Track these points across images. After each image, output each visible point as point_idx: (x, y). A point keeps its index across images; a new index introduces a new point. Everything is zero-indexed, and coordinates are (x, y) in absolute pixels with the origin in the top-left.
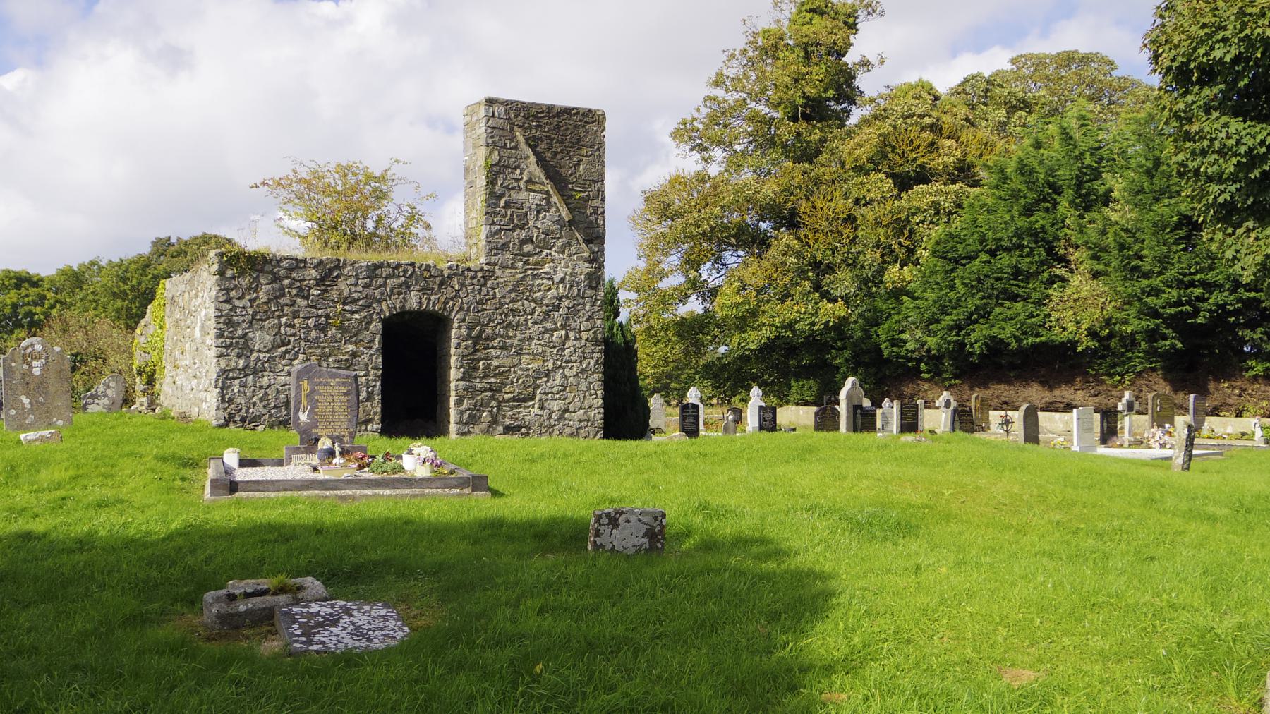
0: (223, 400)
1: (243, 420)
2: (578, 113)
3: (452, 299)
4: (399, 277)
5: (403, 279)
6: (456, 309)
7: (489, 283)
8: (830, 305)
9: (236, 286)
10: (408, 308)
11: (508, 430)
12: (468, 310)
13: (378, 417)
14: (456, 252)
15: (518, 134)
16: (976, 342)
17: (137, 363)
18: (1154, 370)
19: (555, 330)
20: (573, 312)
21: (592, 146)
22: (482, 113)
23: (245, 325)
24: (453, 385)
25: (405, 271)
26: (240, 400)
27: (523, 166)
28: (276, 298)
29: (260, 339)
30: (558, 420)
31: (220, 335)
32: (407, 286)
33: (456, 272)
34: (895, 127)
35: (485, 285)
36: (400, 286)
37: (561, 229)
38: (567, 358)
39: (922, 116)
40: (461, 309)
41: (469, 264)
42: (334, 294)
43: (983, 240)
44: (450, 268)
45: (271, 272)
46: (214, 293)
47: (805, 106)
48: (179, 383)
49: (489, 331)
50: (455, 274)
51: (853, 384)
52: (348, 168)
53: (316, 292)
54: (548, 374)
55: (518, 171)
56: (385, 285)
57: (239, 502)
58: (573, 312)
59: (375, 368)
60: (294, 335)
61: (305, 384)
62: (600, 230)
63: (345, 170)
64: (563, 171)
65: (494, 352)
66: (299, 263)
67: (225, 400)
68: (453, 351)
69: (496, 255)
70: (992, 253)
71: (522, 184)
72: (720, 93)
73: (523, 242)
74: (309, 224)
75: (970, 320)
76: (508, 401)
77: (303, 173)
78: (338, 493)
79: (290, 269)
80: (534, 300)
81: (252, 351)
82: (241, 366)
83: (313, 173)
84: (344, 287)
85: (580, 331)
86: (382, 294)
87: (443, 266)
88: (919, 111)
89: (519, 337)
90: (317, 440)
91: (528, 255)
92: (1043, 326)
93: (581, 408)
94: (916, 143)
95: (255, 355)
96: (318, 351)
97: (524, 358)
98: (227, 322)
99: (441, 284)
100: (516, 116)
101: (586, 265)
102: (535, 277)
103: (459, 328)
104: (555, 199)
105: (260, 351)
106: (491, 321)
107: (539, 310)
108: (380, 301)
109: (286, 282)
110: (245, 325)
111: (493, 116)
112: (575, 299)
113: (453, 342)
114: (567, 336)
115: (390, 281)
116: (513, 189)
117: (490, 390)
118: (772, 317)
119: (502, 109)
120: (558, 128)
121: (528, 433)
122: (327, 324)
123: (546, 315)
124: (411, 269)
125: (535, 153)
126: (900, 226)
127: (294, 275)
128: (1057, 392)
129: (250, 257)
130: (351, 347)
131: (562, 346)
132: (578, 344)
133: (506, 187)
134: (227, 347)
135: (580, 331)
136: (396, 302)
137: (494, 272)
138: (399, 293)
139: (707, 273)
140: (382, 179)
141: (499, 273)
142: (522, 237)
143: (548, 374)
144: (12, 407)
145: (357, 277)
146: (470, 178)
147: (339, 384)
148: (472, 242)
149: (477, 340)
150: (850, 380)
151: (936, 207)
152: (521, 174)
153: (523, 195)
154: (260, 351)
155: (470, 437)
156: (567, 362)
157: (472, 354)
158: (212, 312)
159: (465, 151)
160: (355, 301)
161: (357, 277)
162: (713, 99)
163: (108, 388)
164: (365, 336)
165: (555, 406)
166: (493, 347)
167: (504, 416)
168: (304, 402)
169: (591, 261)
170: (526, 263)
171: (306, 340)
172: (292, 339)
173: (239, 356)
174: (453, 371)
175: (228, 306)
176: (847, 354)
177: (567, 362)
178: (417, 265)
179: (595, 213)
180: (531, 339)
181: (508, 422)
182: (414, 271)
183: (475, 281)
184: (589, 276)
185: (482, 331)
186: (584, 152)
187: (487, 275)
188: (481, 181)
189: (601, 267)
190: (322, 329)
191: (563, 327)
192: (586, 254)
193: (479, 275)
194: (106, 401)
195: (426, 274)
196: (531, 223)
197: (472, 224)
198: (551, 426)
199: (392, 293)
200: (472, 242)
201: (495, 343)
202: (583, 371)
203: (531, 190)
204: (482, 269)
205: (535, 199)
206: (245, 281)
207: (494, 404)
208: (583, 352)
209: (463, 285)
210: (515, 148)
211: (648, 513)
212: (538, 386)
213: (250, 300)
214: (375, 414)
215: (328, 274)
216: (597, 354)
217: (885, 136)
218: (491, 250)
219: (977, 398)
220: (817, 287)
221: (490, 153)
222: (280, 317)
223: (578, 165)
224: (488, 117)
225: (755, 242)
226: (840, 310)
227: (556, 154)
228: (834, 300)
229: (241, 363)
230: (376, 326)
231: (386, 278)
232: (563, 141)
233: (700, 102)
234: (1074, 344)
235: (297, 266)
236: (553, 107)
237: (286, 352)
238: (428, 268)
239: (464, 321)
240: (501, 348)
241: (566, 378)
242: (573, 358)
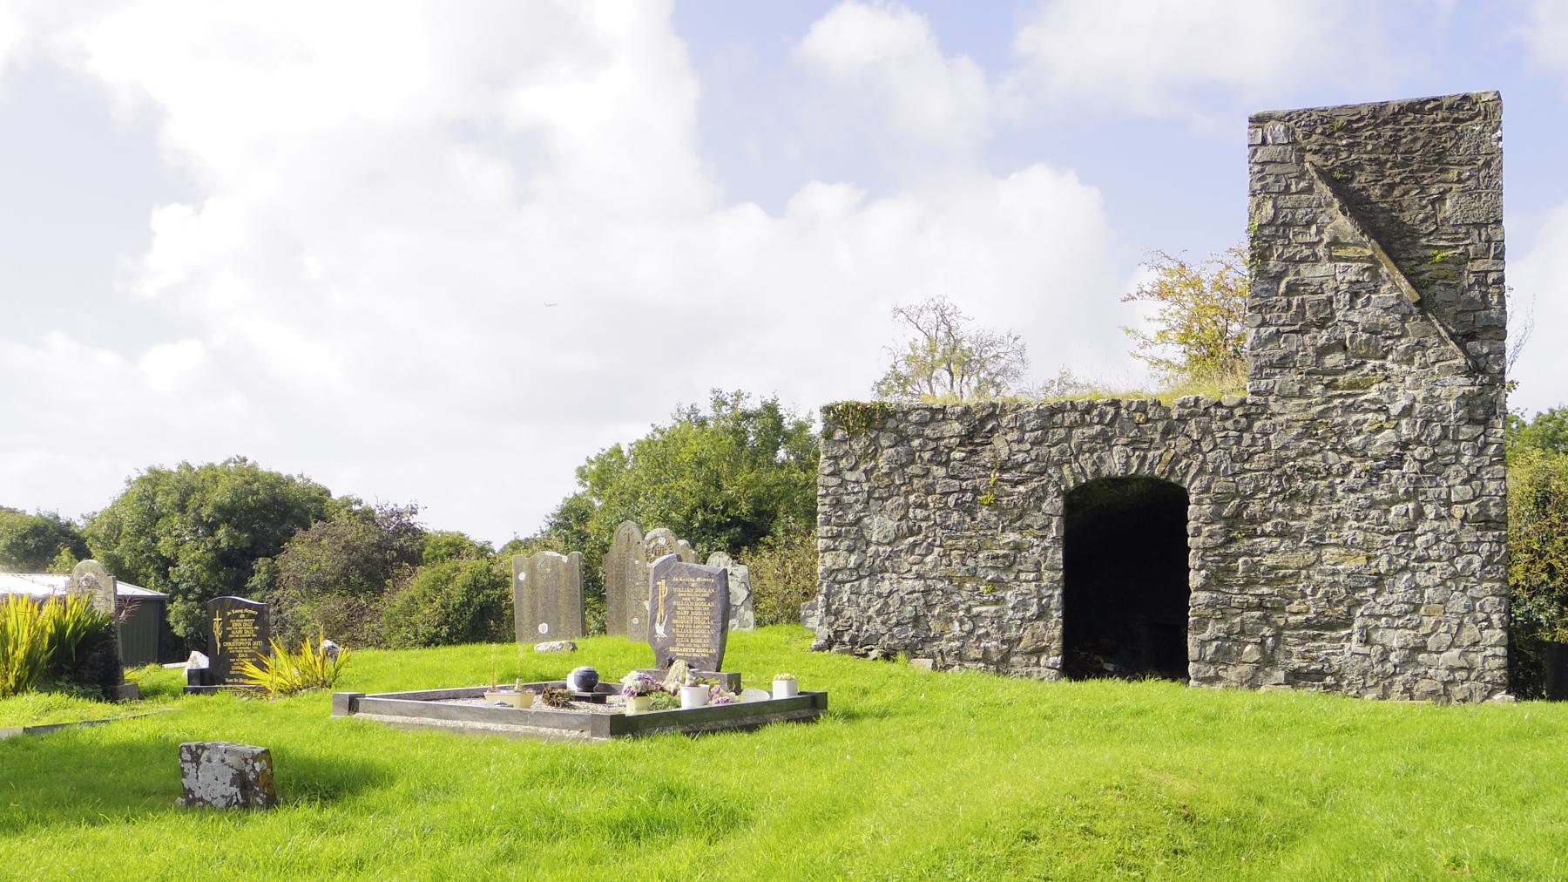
1: (853, 641)
4: (1091, 424)
5: (1098, 428)
6: (1193, 471)
7: (1257, 425)
9: (846, 453)
10: (1105, 472)
11: (1295, 678)
12: (1215, 471)
13: (1056, 645)
19: (1393, 502)
21: (1471, 162)
23: (859, 507)
25: (1102, 415)
27: (1322, 218)
28: (902, 466)
29: (880, 526)
30: (1405, 663)
32: (1106, 439)
35: (1249, 428)
36: (1093, 438)
37: (1404, 319)
38: (1420, 552)
40: (1201, 471)
42: (986, 457)
44: (1183, 405)
45: (896, 430)
50: (1192, 415)
53: (957, 455)
54: (1378, 581)
55: (1314, 228)
56: (1068, 438)
57: (358, 728)
58: (1432, 469)
59: (1052, 568)
60: (926, 519)
62: (1494, 313)
64: (1406, 217)
65: (1266, 543)
69: (1268, 376)
71: (1321, 251)
73: (1323, 351)
76: (1296, 627)
78: (449, 722)
79: (922, 424)
80: (1348, 451)
82: (851, 565)
86: (1063, 453)
89: (1316, 515)
90: (671, 662)
91: (1335, 372)
93: (1452, 645)
95: (873, 548)
96: (962, 543)
97: (1329, 554)
99: (1166, 432)
100: (1307, 136)
101: (1461, 380)
102: (1347, 409)
103: (1199, 502)
105: (878, 543)
106: (1257, 489)
108: (1059, 465)
111: (1264, 142)
114: (1420, 514)
115: (1077, 433)
116: (1303, 260)
117: (1260, 607)
119: (1280, 127)
120: (1396, 140)
121: (1338, 686)
123: (1374, 476)
124: (1111, 410)
127: (928, 432)
130: (1013, 536)
131: (1410, 530)
132: (1443, 526)
133: (1290, 260)
134: (834, 538)
135: (1448, 504)
136: (1087, 462)
137: (1266, 406)
138: (1092, 451)
141: (1275, 407)
142: (1320, 343)
143: (1378, 581)
144: (635, 615)
145: (1022, 428)
147: (701, 585)
152: (1319, 232)
153: (1324, 269)
154: (878, 543)
155: (1219, 687)
156: (1420, 559)
157: (1222, 545)
161: (1022, 428)
164: (1036, 519)
165: (1395, 639)
166: (1263, 534)
167: (1289, 654)
171: (944, 526)
172: (924, 524)
173: (850, 551)
175: (835, 481)
178: (1124, 404)
180: (1339, 518)
181: (1296, 663)
182: (1117, 414)
183: (1229, 424)
184: (1466, 401)
186: (1453, 175)
189: (1498, 380)
190: (970, 511)
191: (1410, 496)
193: (1238, 412)
195: (1138, 417)
196: (1339, 315)
198: (1385, 676)
199: (1080, 451)
201: (1268, 527)
202: (1455, 576)
203: (1340, 259)
207: (1267, 631)
209: (1206, 431)
211: (235, 752)
212: (1359, 603)
213: (865, 471)
214: (1052, 639)
221: (1258, 206)
222: (908, 493)
223: (1441, 198)
227: (1392, 187)
230: (1054, 503)
231: (1071, 428)
235: (933, 419)
236: (1383, 106)
237: (915, 545)
239: (1207, 489)
240: (1278, 535)
242: (1433, 553)
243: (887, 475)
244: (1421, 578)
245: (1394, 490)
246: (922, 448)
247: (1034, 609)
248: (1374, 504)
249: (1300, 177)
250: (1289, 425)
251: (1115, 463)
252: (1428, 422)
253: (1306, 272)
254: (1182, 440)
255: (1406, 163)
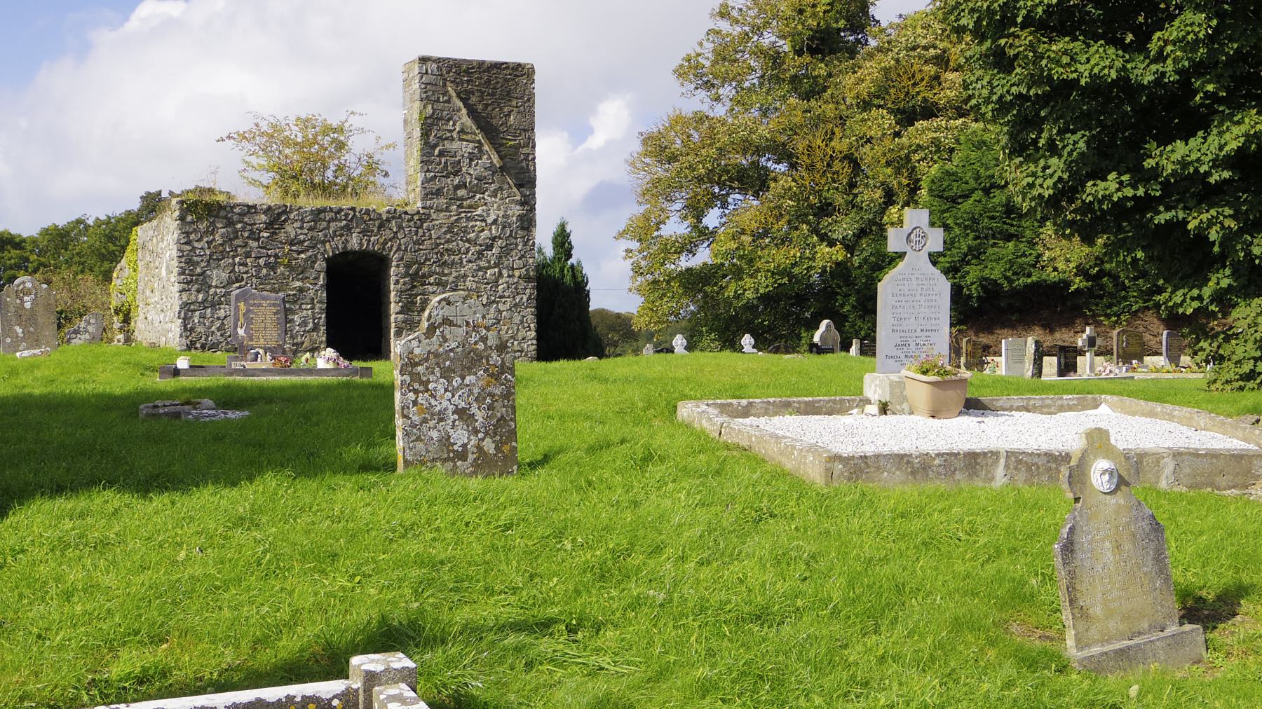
0: (185, 329)
2: (507, 68)
3: (390, 240)
4: (340, 220)
8: (828, 249)
12: (406, 249)
14: (399, 195)
15: (450, 89)
16: (972, 284)
17: (114, 303)
18: (1147, 308)
20: (506, 252)
21: (522, 98)
22: (417, 71)
23: (203, 264)
24: (392, 318)
25: (347, 215)
26: (200, 329)
28: (231, 240)
29: (217, 276)
31: (182, 273)
32: (348, 229)
33: (394, 215)
34: (897, 61)
35: (421, 226)
36: (342, 228)
37: (494, 173)
38: (500, 293)
39: (926, 48)
40: (399, 249)
41: (408, 209)
42: (282, 237)
43: (977, 177)
44: (388, 212)
45: (226, 217)
46: (176, 236)
47: (811, 39)
48: (150, 318)
49: (425, 269)
50: (393, 218)
51: (828, 326)
52: (307, 120)
56: (328, 228)
58: (506, 252)
60: (246, 272)
61: (242, 305)
63: (305, 123)
64: (494, 122)
65: (431, 289)
66: (251, 209)
67: (187, 329)
68: (392, 287)
70: (987, 191)
71: (455, 134)
72: (724, 25)
73: (457, 188)
74: (272, 174)
75: (964, 261)
77: (264, 128)
79: (242, 215)
80: (468, 241)
81: (210, 287)
83: (273, 126)
84: (291, 230)
85: (513, 269)
86: (326, 236)
87: (383, 210)
88: (924, 42)
89: (454, 274)
91: (462, 199)
92: (1034, 266)
94: (918, 76)
98: (188, 262)
99: (380, 227)
100: (448, 73)
101: (518, 207)
102: (468, 219)
103: (398, 266)
104: (486, 147)
105: (217, 287)
106: (427, 260)
107: (473, 250)
108: (324, 243)
109: (239, 226)
110: (203, 264)
111: (427, 73)
112: (507, 239)
113: (393, 279)
114: (500, 274)
115: (333, 225)
118: (767, 262)
119: (435, 66)
120: (489, 81)
122: (276, 263)
123: (480, 254)
124: (352, 213)
125: (466, 105)
126: (902, 163)
128: (1057, 335)
129: (207, 204)
130: (298, 284)
131: (496, 283)
132: (511, 281)
134: (188, 283)
135: (513, 269)
136: (338, 243)
137: (429, 215)
138: (341, 235)
139: (712, 218)
140: (340, 130)
141: (434, 216)
142: (456, 182)
145: (302, 221)
146: (409, 130)
147: (270, 305)
148: (410, 188)
149: (414, 277)
150: (825, 322)
151: (936, 142)
152: (454, 125)
153: (456, 144)
154: (217, 287)
156: (501, 297)
158: (175, 253)
159: (404, 105)
160: (302, 242)
161: (302, 221)
162: (717, 33)
163: (88, 325)
164: (312, 274)
168: (242, 320)
169: (522, 204)
170: (460, 206)
171: (257, 277)
173: (198, 291)
174: (393, 305)
175: (189, 248)
176: (852, 299)
177: (501, 297)
179: (526, 159)
180: (465, 276)
184: (521, 217)
185: (419, 269)
186: (514, 103)
187: (423, 218)
188: (417, 133)
189: (533, 209)
190: (272, 267)
191: (496, 265)
192: (518, 198)
193: (416, 218)
194: (87, 336)
197: (411, 172)
200: (410, 188)
201: (432, 280)
202: (516, 305)
203: (464, 140)
204: (418, 212)
205: (467, 148)
206: (203, 226)
208: (516, 288)
209: (400, 227)
210: (448, 101)
215: (276, 218)
216: (530, 290)
217: (886, 70)
218: (427, 195)
219: (968, 342)
220: (815, 231)
222: (234, 257)
223: (509, 115)
224: (422, 74)
225: (755, 181)
226: (839, 254)
227: (487, 105)
228: (832, 244)
229: (201, 297)
230: (320, 265)
231: (329, 222)
232: (493, 94)
233: (702, 35)
234: (1067, 284)
236: (483, 62)
238: (368, 212)
239: (402, 259)
240: (438, 284)
241: (500, 312)
243: (221, 245)
244: (501, 307)
245: (489, 262)
246: (243, 229)
247: (311, 325)
248: (480, 269)
249: (444, 94)
250: (441, 226)
251: (354, 242)
252: (504, 227)
253: (447, 145)
254: (388, 231)
255: (493, 94)
